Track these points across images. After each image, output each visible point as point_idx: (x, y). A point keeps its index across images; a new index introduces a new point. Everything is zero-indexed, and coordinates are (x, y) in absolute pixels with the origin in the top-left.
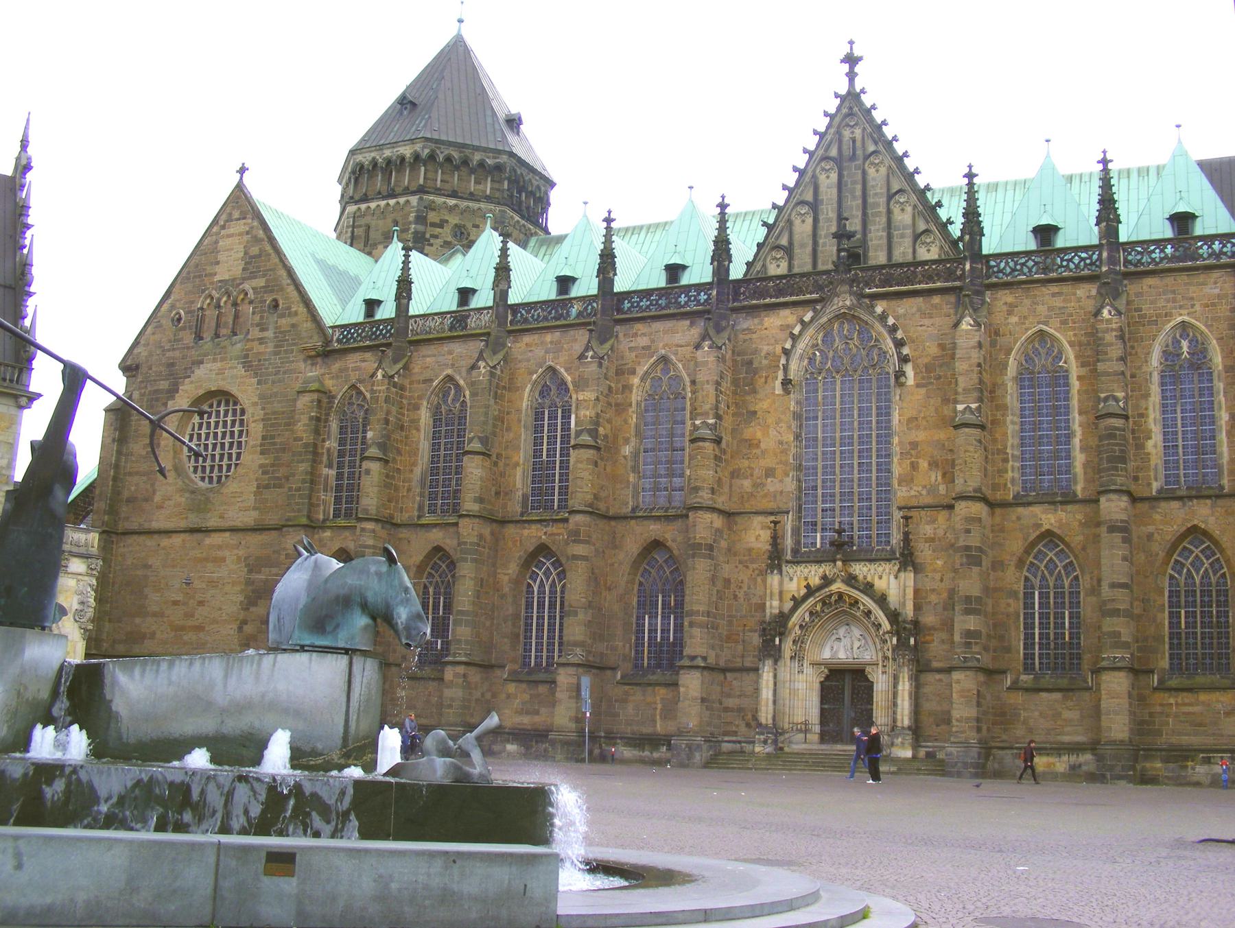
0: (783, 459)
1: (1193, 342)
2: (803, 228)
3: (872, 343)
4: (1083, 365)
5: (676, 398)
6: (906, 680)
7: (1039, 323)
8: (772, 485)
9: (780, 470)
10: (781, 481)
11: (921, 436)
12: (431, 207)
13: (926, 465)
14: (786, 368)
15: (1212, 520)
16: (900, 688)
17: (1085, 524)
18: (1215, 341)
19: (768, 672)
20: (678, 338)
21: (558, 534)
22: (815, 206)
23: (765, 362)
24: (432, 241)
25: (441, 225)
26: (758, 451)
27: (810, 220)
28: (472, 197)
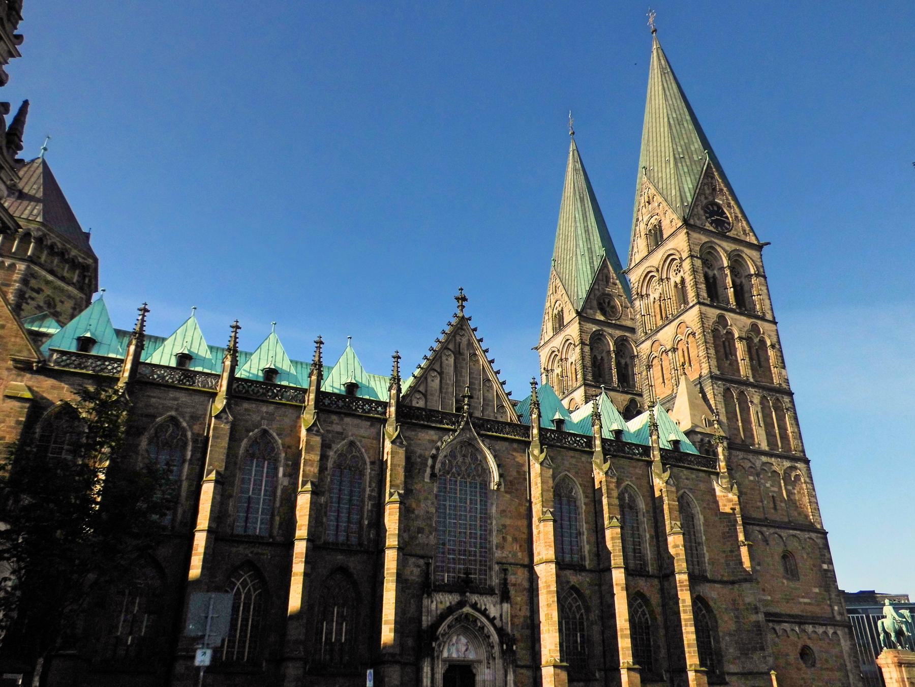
0: (429, 522)
1: (630, 496)
2: (435, 384)
3: (479, 462)
4: (587, 497)
5: (356, 470)
6: (512, 673)
7: (565, 470)
8: (422, 538)
9: (427, 530)
10: (428, 537)
11: (508, 522)
12: (34, 276)
13: (511, 539)
14: (433, 467)
15: (645, 588)
16: (508, 678)
17: (590, 584)
18: (641, 497)
19: (427, 667)
20: (362, 432)
21: (263, 554)
22: (441, 374)
23: (419, 460)
24: (29, 301)
25: (38, 291)
26: (413, 516)
27: (437, 381)
28: (63, 279)
